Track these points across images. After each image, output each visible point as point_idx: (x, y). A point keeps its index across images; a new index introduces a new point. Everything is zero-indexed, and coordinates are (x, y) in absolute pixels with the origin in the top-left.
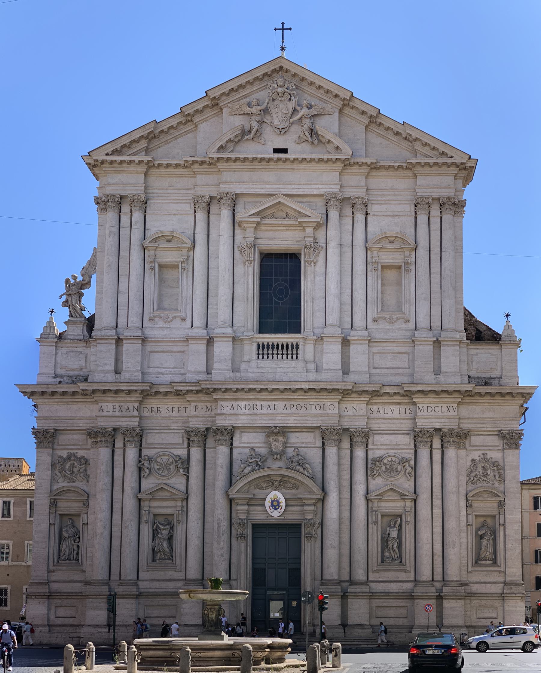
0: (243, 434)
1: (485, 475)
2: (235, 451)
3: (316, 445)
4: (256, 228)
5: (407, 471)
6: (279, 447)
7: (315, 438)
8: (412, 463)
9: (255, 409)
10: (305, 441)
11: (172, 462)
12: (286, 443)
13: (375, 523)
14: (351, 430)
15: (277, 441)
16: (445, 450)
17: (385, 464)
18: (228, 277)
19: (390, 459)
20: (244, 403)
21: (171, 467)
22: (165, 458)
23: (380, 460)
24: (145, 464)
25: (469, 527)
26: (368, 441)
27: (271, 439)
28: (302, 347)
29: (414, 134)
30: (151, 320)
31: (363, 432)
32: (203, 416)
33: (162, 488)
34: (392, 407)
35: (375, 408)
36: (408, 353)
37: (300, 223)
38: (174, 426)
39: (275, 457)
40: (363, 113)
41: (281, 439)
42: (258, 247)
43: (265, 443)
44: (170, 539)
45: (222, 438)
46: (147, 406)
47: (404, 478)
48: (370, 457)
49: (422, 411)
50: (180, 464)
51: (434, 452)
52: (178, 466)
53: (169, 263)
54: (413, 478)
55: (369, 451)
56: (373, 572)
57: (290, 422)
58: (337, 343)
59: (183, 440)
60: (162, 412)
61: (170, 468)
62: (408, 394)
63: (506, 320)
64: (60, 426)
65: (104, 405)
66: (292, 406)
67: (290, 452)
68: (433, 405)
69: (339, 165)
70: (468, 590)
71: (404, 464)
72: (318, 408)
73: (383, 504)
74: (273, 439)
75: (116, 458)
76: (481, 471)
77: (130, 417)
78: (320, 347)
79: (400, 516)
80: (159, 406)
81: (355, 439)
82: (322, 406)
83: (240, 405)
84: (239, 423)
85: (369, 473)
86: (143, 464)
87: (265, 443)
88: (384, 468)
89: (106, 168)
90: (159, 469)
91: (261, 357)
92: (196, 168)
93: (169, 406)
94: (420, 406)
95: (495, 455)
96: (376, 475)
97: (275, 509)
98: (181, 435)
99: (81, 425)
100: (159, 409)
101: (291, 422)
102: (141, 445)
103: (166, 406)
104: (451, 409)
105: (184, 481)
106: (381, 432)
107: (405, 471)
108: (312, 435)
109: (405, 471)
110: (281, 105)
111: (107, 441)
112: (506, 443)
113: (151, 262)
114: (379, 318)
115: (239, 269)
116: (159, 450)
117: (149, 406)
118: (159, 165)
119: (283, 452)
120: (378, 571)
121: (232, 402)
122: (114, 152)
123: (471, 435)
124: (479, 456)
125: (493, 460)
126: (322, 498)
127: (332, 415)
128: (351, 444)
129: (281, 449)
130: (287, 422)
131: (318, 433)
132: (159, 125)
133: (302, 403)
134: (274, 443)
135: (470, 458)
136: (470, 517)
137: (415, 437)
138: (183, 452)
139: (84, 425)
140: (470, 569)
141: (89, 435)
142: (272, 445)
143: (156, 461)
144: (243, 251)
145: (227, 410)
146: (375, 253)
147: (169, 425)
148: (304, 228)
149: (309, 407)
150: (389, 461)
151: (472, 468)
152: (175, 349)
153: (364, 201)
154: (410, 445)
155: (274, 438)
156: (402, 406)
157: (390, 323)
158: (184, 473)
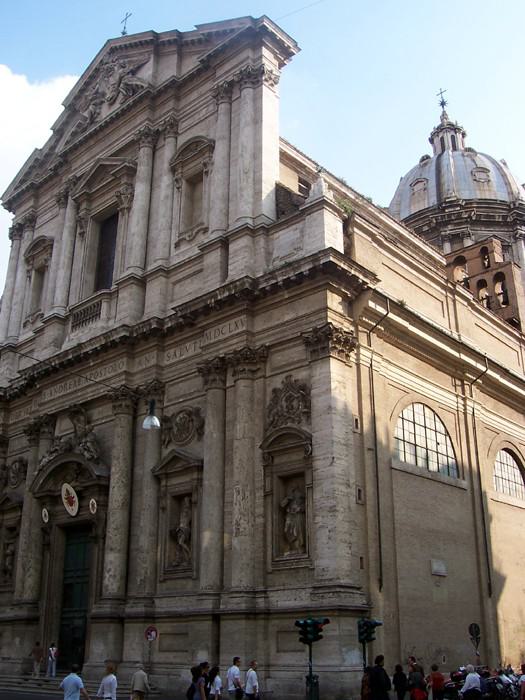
1: (290, 408)
10: (105, 414)
13: (164, 509)
19: (181, 415)
20: (58, 386)
25: (269, 499)
35: (172, 351)
36: (201, 271)
41: (82, 418)
44: (13, 554)
56: (161, 582)
69: (147, 102)
70: (261, 603)
73: (174, 481)
76: (284, 404)
79: (190, 495)
89: (14, 205)
95: (301, 375)
97: (71, 505)
101: (89, 395)
104: (239, 324)
112: (314, 351)
120: (165, 580)
122: (15, 189)
123: (272, 353)
124: (283, 382)
125: (300, 383)
135: (269, 390)
136: (268, 480)
140: (270, 568)
145: (47, 398)
157: (189, 241)
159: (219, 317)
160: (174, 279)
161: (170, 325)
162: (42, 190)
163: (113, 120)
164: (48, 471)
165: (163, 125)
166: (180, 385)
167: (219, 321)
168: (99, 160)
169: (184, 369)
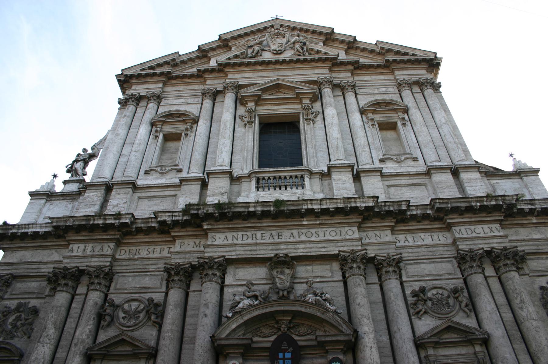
0: (237, 270)
2: (226, 290)
3: (335, 279)
4: (257, 104)
5: (463, 305)
6: (286, 282)
7: (332, 272)
8: (466, 294)
9: (254, 239)
11: (143, 309)
12: (293, 277)
14: (379, 258)
15: (282, 273)
16: (503, 276)
17: (430, 299)
18: (229, 132)
19: (434, 292)
20: (240, 234)
21: (142, 315)
22: (134, 305)
23: (423, 290)
24: (107, 311)
26: (400, 271)
27: (275, 273)
28: (308, 179)
29: (387, 47)
30: (147, 173)
31: (394, 260)
32: (189, 252)
33: (123, 340)
34: (422, 235)
36: (424, 184)
37: (297, 94)
38: (153, 268)
39: (281, 293)
40: (342, 42)
41: (287, 271)
42: (258, 115)
43: (266, 279)
45: (210, 272)
46: (124, 248)
47: (461, 314)
48: (408, 292)
49: (460, 233)
50: (153, 309)
51: (490, 280)
52: (150, 312)
53: (174, 132)
54: (473, 314)
55: (405, 284)
57: (299, 251)
58: (347, 173)
59: (161, 283)
60: (142, 254)
61: (139, 316)
62: (441, 215)
63: (514, 156)
64: (21, 272)
65: (75, 247)
66: (301, 234)
67: (300, 289)
68: (473, 227)
71: (457, 295)
72: (333, 234)
74: (277, 272)
75: (73, 305)
77: (102, 256)
78: (327, 182)
80: (138, 248)
81: (384, 270)
82: (338, 232)
83: (236, 236)
84: (232, 254)
85: (412, 311)
86: (105, 311)
87: (266, 279)
88: (429, 303)
90: (123, 318)
91: (261, 189)
92: (207, 75)
93: (150, 247)
94: (457, 228)
96: (422, 313)
98: (160, 277)
99: (43, 270)
100: (138, 250)
101: (301, 250)
102: (108, 291)
103: (147, 247)
105: (154, 332)
106: (416, 261)
107: (460, 305)
108: (328, 267)
109: (460, 305)
110: (278, 39)
111: (66, 285)
113: (157, 131)
114: (386, 159)
115: (240, 130)
116: (129, 295)
117: (127, 249)
118: (177, 77)
119: (290, 290)
121: (226, 234)
126: (353, 340)
127: (353, 240)
128: (380, 278)
129: (288, 284)
130: (295, 251)
131: (336, 266)
132: (181, 57)
133: (313, 231)
134: (279, 276)
135: (537, 286)
137: (459, 263)
138: (158, 297)
139: (46, 270)
141: (49, 281)
142: (277, 279)
143: (123, 308)
144: (244, 118)
146: (370, 115)
147: (147, 267)
148: (301, 100)
149: (321, 234)
150: (434, 295)
151: (545, 297)
152: (167, 193)
153: (352, 85)
154: (455, 274)
155: (279, 270)
156: (433, 234)
158: (156, 320)
159: (473, 220)
160: (388, 183)
161: (415, 213)
162: (173, 82)
163: (269, 63)
164: (246, 318)
165: (344, 83)
166: (423, 266)
167: (471, 223)
168: (278, 80)
169: (424, 254)
